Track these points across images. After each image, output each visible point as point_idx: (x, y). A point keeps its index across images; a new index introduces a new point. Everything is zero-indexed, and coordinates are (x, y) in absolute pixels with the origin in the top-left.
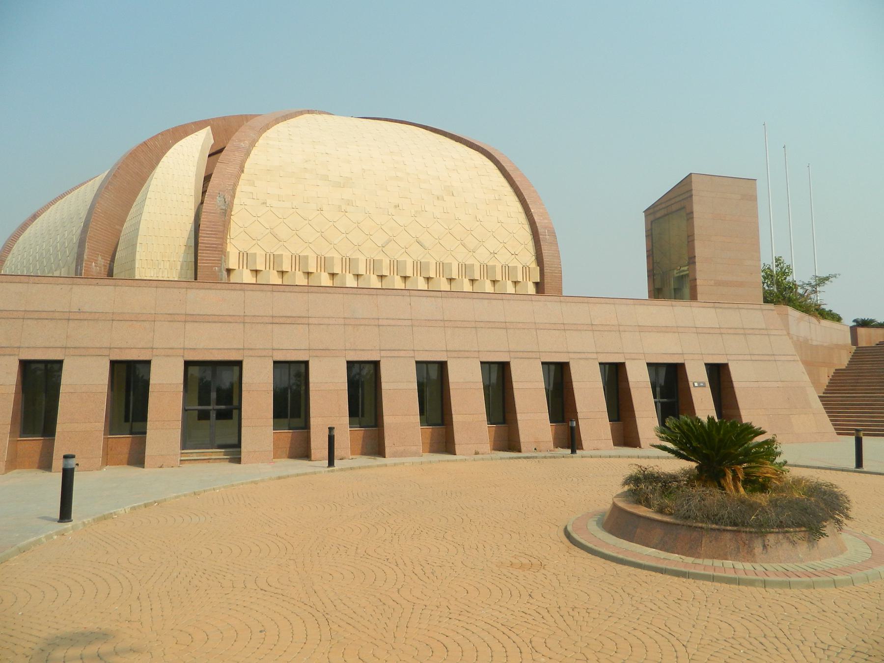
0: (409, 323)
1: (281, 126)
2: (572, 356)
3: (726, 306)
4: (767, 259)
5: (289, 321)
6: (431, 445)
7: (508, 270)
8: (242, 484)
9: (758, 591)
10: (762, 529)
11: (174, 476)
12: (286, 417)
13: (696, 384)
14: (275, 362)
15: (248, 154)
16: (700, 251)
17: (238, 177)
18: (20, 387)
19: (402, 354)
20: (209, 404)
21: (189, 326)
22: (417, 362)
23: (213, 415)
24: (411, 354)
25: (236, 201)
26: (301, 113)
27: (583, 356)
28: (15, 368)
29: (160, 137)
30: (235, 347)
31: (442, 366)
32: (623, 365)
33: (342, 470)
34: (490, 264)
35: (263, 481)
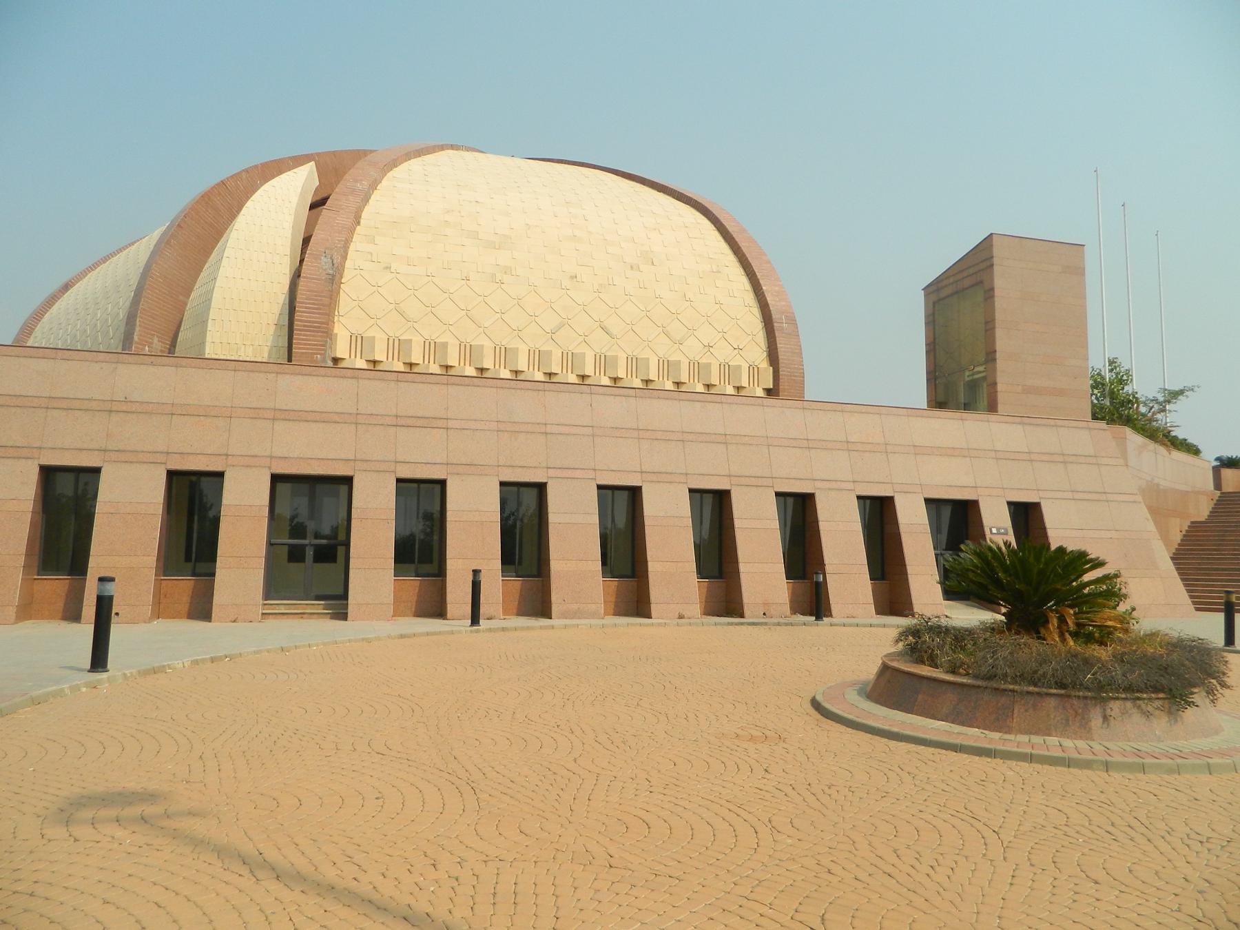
0: (589, 431)
1: (415, 164)
2: (818, 484)
3: (1039, 421)
4: (1097, 361)
5: (419, 423)
7: (729, 371)
8: (350, 641)
9: (1098, 776)
11: (250, 631)
12: (412, 562)
13: (994, 531)
14: (399, 481)
15: (366, 200)
16: (1003, 343)
17: (352, 231)
18: (40, 506)
19: (578, 474)
20: (305, 538)
21: (279, 426)
22: (600, 487)
23: (310, 553)
24: (591, 474)
25: (348, 264)
26: (442, 148)
27: (834, 485)
28: (34, 476)
29: (244, 175)
30: (343, 457)
31: (634, 493)
32: (890, 500)
34: (703, 361)
35: (378, 639)
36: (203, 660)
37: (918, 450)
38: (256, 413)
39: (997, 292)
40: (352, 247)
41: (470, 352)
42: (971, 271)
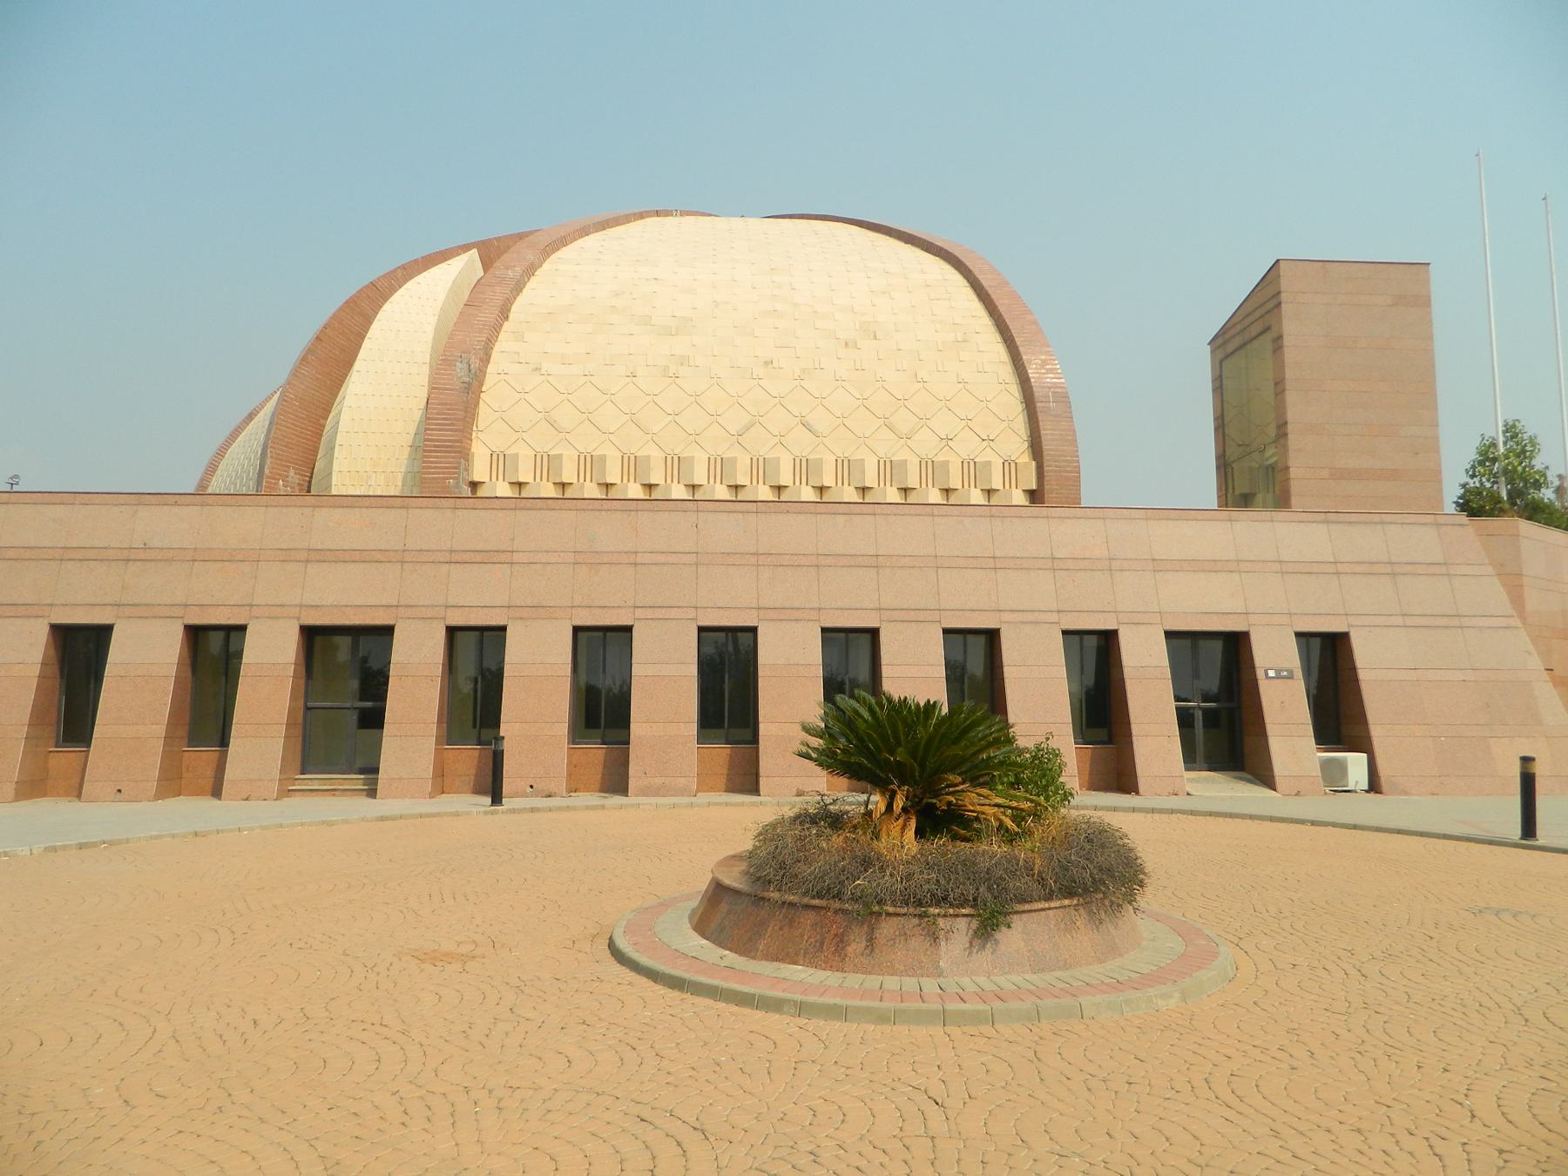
0: (692, 558)
1: (592, 241)
2: (1006, 617)
3: (1354, 517)
5: (479, 558)
6: (730, 779)
7: (974, 470)
8: (302, 824)
10: (870, 910)
13: (1271, 673)
15: (518, 288)
16: (1297, 410)
17: (497, 328)
18: (54, 670)
21: (312, 569)
25: (491, 369)
26: (641, 216)
27: (1030, 617)
33: (513, 811)
36: (65, 848)
37: (1158, 565)
39: (1287, 341)
40: (497, 348)
41: (633, 465)
42: (1258, 314)
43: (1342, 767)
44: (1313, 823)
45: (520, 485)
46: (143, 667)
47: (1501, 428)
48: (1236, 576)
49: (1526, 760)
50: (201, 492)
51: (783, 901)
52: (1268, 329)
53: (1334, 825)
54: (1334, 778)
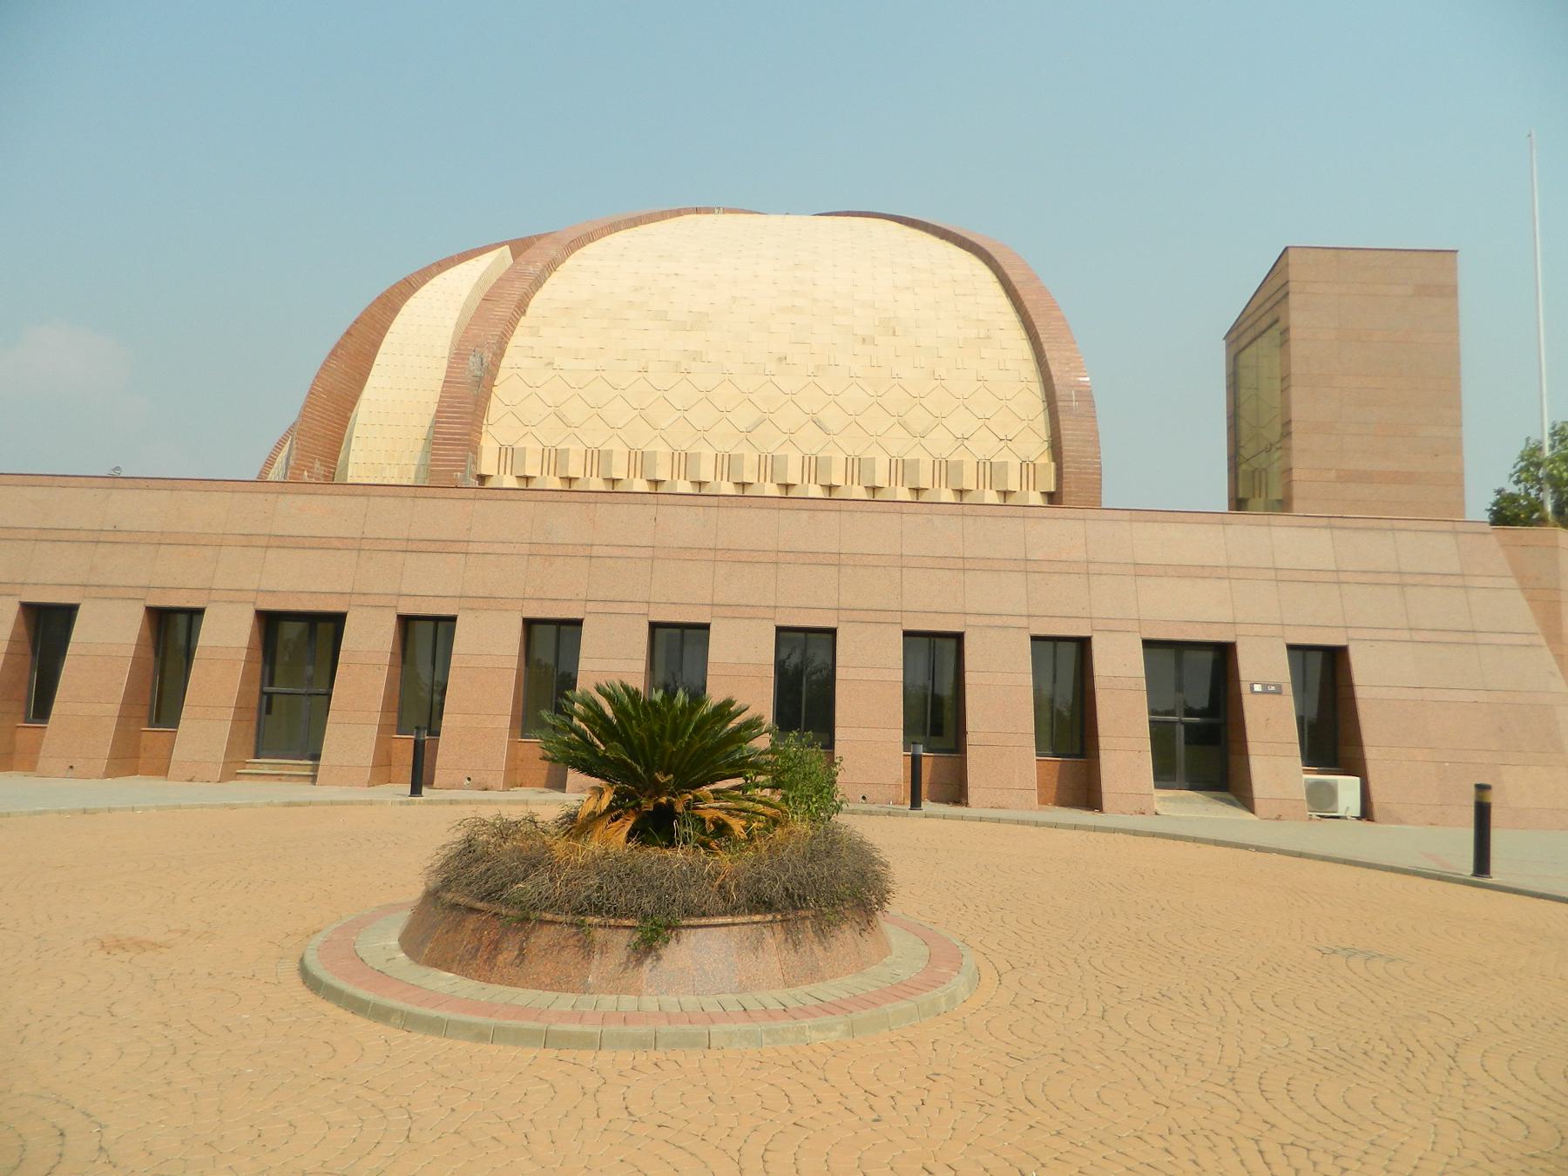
0: (649, 552)
2: (971, 620)
3: (1361, 523)
5: (433, 547)
7: (990, 470)
8: (202, 806)
10: (526, 918)
13: (1257, 688)
15: (538, 282)
16: (1301, 410)
17: (512, 324)
18: (26, 648)
19: (626, 608)
21: (272, 554)
24: (644, 608)
25: (505, 362)
26: (679, 213)
27: (998, 621)
30: (339, 589)
33: (430, 802)
34: (954, 458)
37: (1141, 570)
38: (248, 541)
39: (1293, 333)
41: (640, 460)
42: (1268, 305)
43: (1331, 791)
44: (1259, 849)
45: (527, 478)
46: (106, 644)
47: (1547, 430)
48: (1226, 583)
49: (1482, 788)
50: (262, 479)
51: (485, 906)
52: (1276, 321)
53: (1280, 852)
54: (1322, 801)
